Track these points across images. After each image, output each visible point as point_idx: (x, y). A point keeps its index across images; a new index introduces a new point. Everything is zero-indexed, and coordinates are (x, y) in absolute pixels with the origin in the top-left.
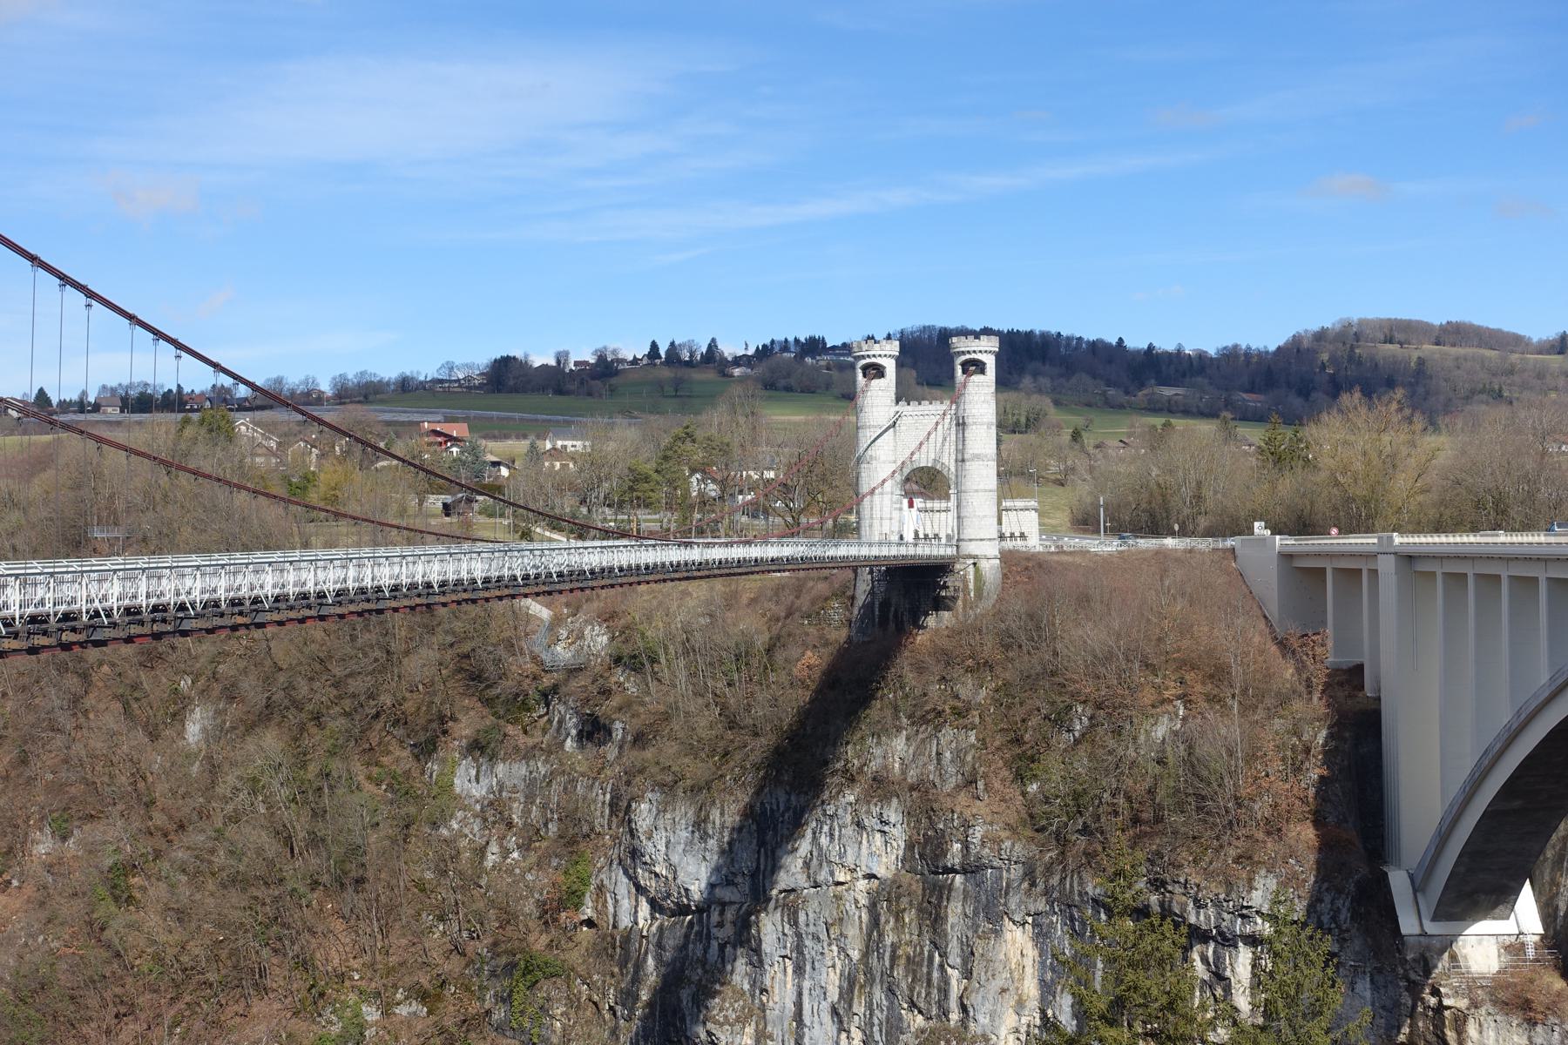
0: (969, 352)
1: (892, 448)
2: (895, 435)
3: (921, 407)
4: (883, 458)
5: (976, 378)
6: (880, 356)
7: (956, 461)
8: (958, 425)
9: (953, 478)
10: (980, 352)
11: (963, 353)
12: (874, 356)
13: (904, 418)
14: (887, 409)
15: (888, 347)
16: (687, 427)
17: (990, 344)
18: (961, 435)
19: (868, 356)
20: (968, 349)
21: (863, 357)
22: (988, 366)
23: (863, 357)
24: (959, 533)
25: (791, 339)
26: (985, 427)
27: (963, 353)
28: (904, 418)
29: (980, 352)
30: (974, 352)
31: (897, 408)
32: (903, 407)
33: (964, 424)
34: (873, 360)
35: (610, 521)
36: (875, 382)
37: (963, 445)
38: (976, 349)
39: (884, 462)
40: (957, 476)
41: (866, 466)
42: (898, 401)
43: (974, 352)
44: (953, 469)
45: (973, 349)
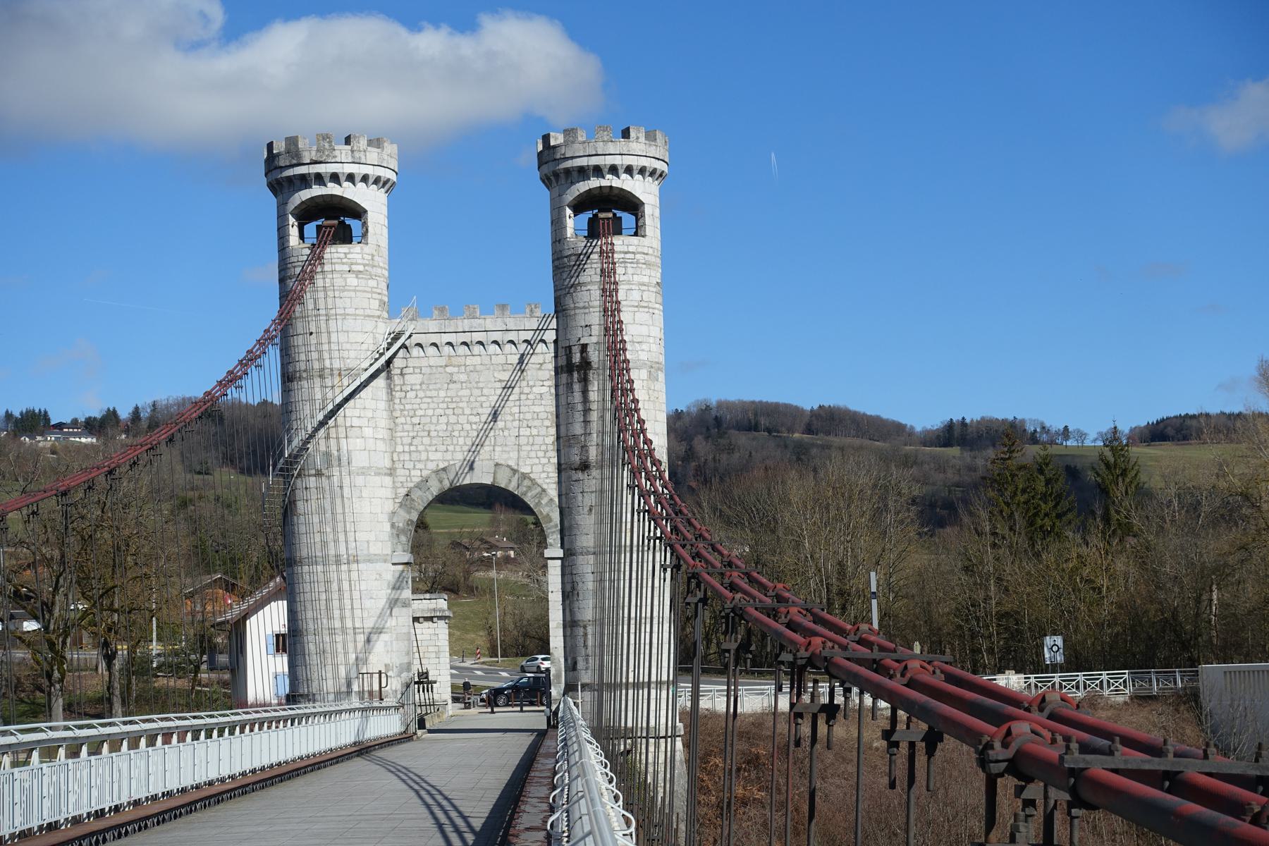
0: (598, 171)
1: (382, 433)
2: (391, 399)
4: (359, 460)
5: (620, 243)
6: (351, 178)
7: (560, 469)
10: (629, 170)
11: (583, 173)
12: (335, 178)
14: (369, 325)
15: (373, 155)
17: (653, 151)
18: (577, 397)
19: (319, 179)
20: (594, 161)
21: (304, 181)
22: (648, 210)
23: (304, 181)
27: (583, 173)
28: (416, 352)
29: (629, 170)
33: (586, 365)
34: (332, 189)
36: (335, 252)
38: (617, 160)
39: (364, 472)
41: (312, 482)
43: (614, 170)
44: (553, 492)
45: (609, 161)
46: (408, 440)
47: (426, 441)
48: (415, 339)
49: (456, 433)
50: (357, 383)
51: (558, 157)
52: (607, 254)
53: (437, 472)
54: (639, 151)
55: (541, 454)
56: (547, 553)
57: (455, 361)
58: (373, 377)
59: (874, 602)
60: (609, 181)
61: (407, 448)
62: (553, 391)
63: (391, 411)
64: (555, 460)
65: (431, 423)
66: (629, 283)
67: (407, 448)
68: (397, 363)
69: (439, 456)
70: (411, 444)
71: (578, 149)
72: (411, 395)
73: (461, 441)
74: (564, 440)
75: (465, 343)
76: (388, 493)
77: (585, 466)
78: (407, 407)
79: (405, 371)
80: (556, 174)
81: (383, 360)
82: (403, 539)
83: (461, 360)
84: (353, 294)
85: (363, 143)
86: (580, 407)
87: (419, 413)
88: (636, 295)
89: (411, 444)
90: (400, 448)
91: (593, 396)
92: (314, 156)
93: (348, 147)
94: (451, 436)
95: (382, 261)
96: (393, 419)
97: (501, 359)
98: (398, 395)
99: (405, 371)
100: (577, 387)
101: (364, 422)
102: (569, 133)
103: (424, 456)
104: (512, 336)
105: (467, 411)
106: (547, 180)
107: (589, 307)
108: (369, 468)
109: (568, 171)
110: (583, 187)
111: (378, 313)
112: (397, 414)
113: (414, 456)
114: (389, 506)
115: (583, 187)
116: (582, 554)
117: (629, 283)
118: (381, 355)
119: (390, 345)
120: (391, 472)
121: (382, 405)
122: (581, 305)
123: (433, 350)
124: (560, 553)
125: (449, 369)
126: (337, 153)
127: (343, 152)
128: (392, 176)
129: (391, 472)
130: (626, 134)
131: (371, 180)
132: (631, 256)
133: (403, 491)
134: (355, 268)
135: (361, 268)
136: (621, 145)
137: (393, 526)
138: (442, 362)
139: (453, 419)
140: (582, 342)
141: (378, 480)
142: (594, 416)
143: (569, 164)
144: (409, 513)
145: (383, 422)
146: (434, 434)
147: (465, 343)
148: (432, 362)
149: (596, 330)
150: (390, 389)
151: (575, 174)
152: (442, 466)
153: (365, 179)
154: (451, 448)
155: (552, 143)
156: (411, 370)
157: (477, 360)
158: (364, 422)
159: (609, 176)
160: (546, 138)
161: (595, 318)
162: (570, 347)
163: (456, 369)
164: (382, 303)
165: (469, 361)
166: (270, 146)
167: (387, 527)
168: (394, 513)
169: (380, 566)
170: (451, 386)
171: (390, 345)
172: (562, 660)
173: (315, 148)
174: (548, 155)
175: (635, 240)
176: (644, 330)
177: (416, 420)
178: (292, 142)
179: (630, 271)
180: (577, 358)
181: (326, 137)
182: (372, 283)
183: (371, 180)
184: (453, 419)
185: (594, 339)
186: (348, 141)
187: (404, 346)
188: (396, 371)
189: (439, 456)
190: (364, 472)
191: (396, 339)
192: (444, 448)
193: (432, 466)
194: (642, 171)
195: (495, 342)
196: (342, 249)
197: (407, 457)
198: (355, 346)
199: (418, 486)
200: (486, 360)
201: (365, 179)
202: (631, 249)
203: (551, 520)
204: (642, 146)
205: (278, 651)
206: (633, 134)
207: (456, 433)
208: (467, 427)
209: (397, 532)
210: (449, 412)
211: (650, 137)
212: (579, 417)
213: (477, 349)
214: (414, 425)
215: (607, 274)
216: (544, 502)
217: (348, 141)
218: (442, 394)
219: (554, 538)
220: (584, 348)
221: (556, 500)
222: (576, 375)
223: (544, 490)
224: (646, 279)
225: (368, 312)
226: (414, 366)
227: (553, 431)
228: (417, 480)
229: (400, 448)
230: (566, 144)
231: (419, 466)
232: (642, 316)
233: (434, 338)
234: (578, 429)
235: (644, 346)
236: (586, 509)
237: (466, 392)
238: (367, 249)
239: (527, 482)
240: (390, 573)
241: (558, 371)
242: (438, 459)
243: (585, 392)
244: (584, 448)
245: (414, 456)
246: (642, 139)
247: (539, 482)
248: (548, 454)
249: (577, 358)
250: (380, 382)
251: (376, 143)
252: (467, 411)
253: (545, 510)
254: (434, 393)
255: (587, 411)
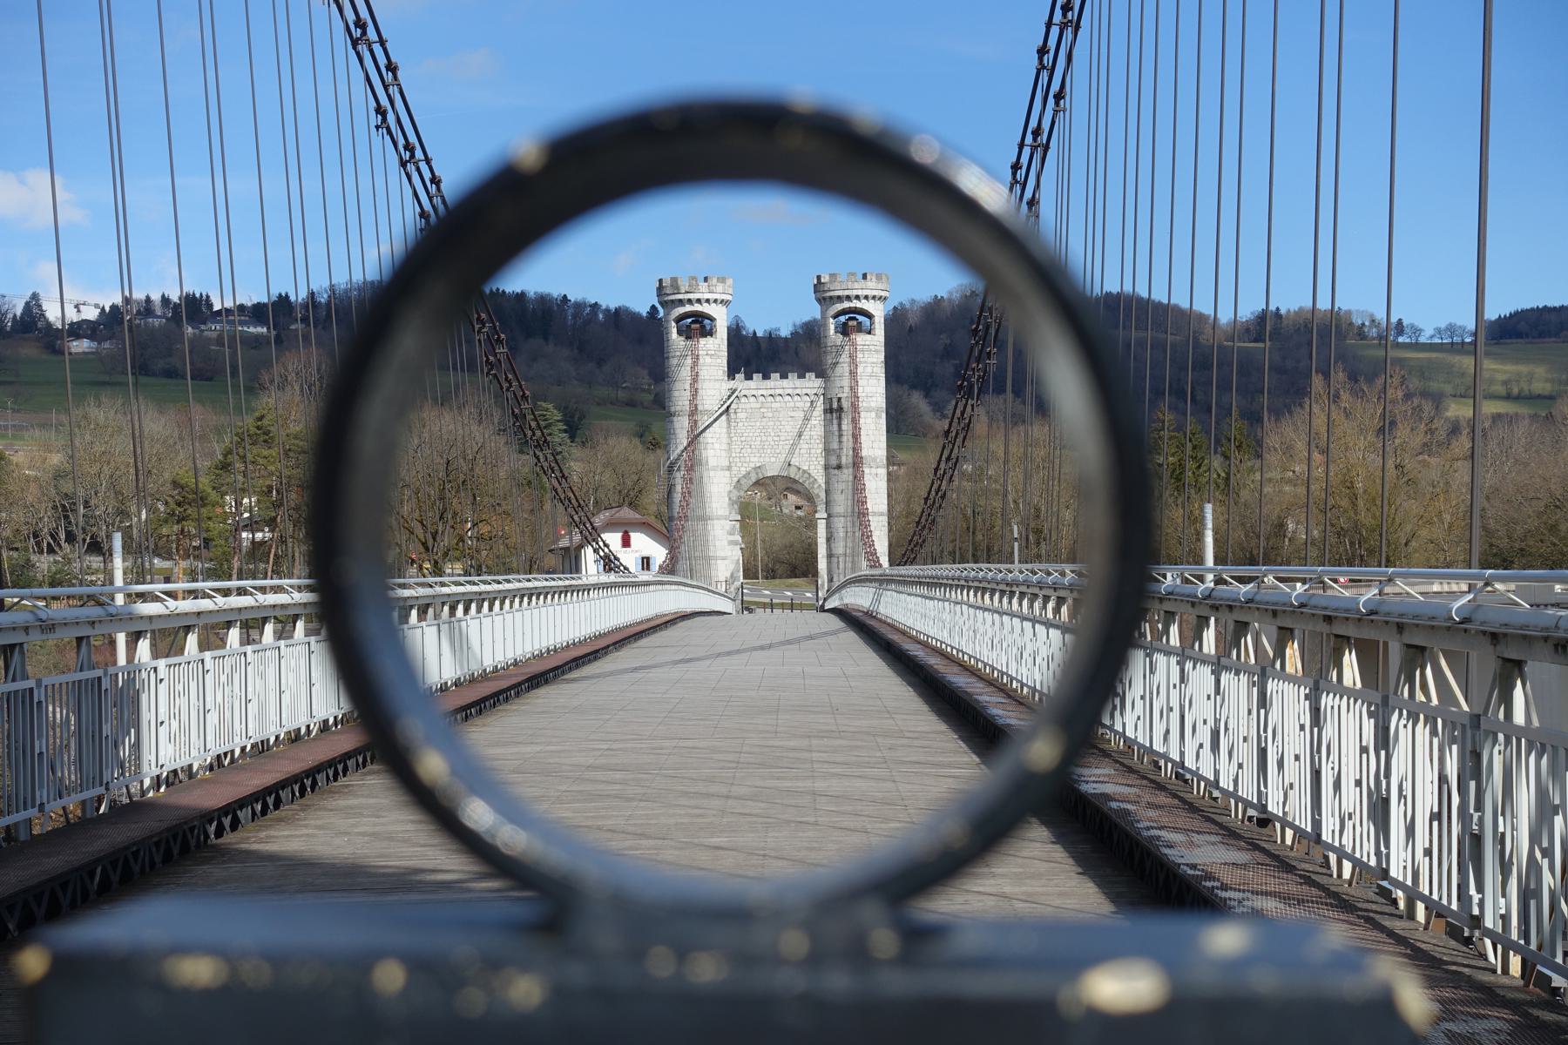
0: (848, 298)
1: (725, 447)
2: (729, 426)
3: (768, 383)
4: (712, 462)
5: (861, 339)
6: (708, 301)
7: (827, 467)
8: (829, 411)
9: (823, 495)
10: (866, 297)
12: (699, 301)
13: (743, 400)
14: (717, 385)
15: (720, 288)
16: (261, 418)
17: (880, 286)
18: (835, 427)
19: (690, 301)
20: (847, 293)
21: (681, 302)
23: (681, 302)
24: (831, 580)
25: (156, 297)
26: (873, 414)
28: (743, 400)
29: (866, 297)
30: (857, 297)
31: (732, 384)
32: (740, 382)
33: (840, 409)
35: (97, 571)
37: (840, 442)
38: (859, 293)
39: (715, 468)
40: (827, 492)
42: (732, 372)
43: (857, 297)
44: (821, 480)
45: (855, 293)
46: (738, 450)
47: (749, 450)
48: (743, 392)
49: (766, 447)
50: (712, 419)
51: (826, 289)
52: (854, 345)
53: (755, 468)
54: (872, 287)
55: (814, 459)
56: (817, 516)
57: (765, 405)
58: (721, 415)
59: (1016, 544)
60: (855, 304)
61: (738, 455)
62: (822, 423)
63: (729, 433)
64: (823, 463)
65: (752, 441)
66: (866, 362)
67: (738, 455)
68: (733, 406)
69: (756, 459)
70: (740, 453)
71: (836, 285)
72: (740, 424)
73: (769, 451)
74: (828, 451)
75: (771, 395)
76: (728, 480)
77: (839, 467)
78: (739, 431)
79: (737, 411)
80: (824, 299)
81: (725, 406)
82: (736, 506)
83: (769, 405)
84: (708, 368)
85: (715, 281)
86: (837, 433)
87: (745, 434)
88: (869, 370)
89: (740, 453)
90: (734, 455)
91: (844, 427)
92: (687, 289)
93: (706, 284)
94: (763, 449)
95: (724, 347)
96: (730, 438)
97: (792, 404)
98: (733, 424)
99: (737, 411)
100: (835, 422)
101: (714, 440)
102: (833, 276)
103: (748, 459)
104: (798, 391)
105: (773, 434)
106: (819, 300)
107: (842, 376)
108: (717, 466)
109: (831, 298)
110: (839, 307)
111: (722, 378)
112: (732, 435)
113: (742, 459)
114: (728, 488)
115: (839, 307)
116: (837, 516)
117: (866, 362)
118: (725, 402)
119: (730, 397)
120: (729, 468)
121: (725, 430)
122: (838, 374)
123: (753, 399)
124: (825, 516)
125: (762, 410)
126: (700, 287)
127: (703, 286)
128: (729, 297)
129: (729, 468)
130: (865, 276)
131: (719, 302)
132: (866, 347)
133: (736, 479)
134: (709, 352)
135: (713, 352)
136: (862, 283)
137: (730, 499)
138: (758, 405)
139: (764, 439)
140: (839, 396)
141: (722, 473)
142: (844, 439)
143: (831, 294)
144: (739, 491)
145: (725, 440)
146: (753, 447)
147: (771, 395)
148: (754, 405)
149: (847, 389)
150: (729, 421)
151: (835, 299)
152: (758, 465)
153: (715, 301)
154: (763, 455)
155: (822, 281)
156: (740, 410)
157: (778, 405)
158: (714, 440)
159: (855, 301)
160: (819, 278)
161: (846, 382)
162: (831, 399)
163: (765, 410)
164: (724, 371)
165: (774, 405)
166: (661, 281)
167: (727, 499)
168: (730, 492)
169: (723, 522)
170: (764, 419)
171: (730, 397)
172: (826, 576)
173: (688, 284)
174: (819, 287)
175: (869, 337)
176: (874, 390)
177: (743, 439)
178: (674, 280)
179: (866, 356)
180: (835, 405)
181: (694, 278)
182: (719, 361)
183: (719, 302)
184: (764, 439)
185: (845, 395)
186: (706, 279)
187: (737, 397)
188: (731, 411)
189: (756, 459)
190: (715, 468)
191: (733, 393)
192: (759, 455)
193: (752, 465)
194: (874, 297)
195: (789, 395)
196: (703, 341)
197: (738, 460)
198: (711, 397)
199: (744, 477)
200: (783, 405)
201: (715, 301)
202: (867, 343)
203: (819, 497)
204: (874, 284)
205: (643, 569)
206: (868, 277)
207: (766, 447)
208: (772, 443)
209: (732, 502)
210: (762, 434)
211: (879, 277)
212: (836, 439)
213: (778, 398)
214: (742, 441)
215: (853, 357)
216: (816, 486)
217: (706, 279)
218: (758, 424)
219: (821, 507)
220: (839, 399)
221: (823, 486)
222: (834, 415)
223: (816, 480)
224: (875, 360)
225: (717, 378)
226: (743, 408)
227: (821, 446)
228: (744, 473)
229: (734, 455)
230: (831, 282)
231: (745, 465)
232: (873, 381)
233: (754, 392)
234: (835, 445)
235: (874, 399)
236: (840, 491)
237: (772, 423)
238: (717, 341)
239: (806, 475)
240: (728, 525)
241: (825, 411)
242: (755, 461)
243: (840, 425)
244: (839, 457)
245: (742, 459)
246: (874, 279)
247: (813, 475)
248: (819, 459)
249: (835, 405)
250: (724, 417)
251: (722, 280)
252: (773, 434)
253: (816, 491)
254: (753, 424)
255: (840, 436)
